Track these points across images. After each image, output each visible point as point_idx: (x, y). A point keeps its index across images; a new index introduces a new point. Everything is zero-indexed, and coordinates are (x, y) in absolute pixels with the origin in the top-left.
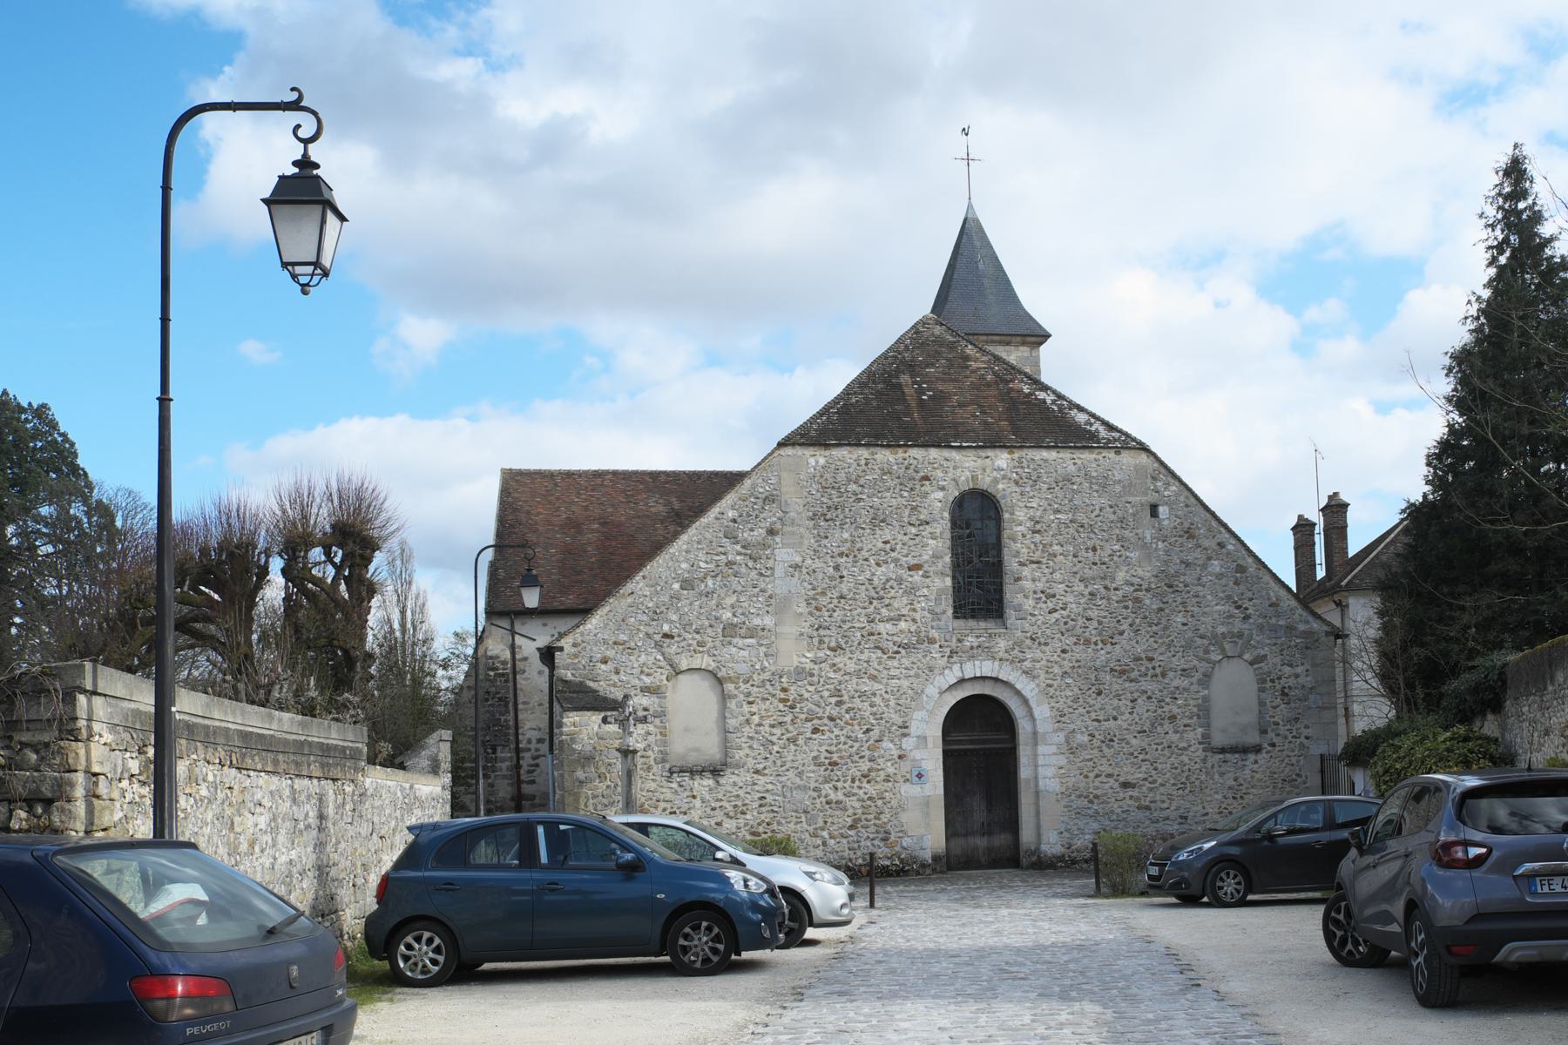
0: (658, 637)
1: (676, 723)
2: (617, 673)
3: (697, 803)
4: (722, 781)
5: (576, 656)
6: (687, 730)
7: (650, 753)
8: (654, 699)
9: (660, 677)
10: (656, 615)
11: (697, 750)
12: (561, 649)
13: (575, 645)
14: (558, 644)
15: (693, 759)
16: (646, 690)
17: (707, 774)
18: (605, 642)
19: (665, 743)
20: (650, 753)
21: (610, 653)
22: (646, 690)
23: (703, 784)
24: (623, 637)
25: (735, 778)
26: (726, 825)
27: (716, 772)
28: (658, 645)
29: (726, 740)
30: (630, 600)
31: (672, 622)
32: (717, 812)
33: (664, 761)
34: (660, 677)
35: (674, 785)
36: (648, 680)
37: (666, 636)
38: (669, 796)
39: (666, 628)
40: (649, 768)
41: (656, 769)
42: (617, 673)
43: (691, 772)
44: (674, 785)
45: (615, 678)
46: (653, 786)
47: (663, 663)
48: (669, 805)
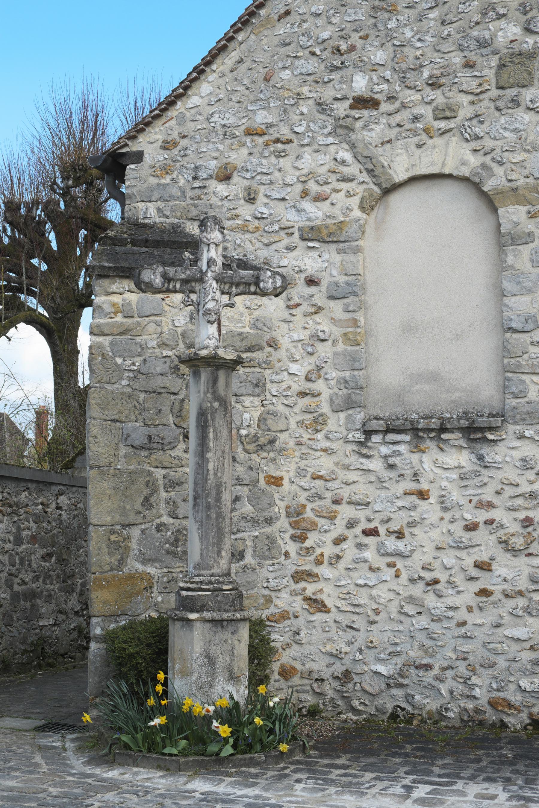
0: (342, 108)
1: (384, 313)
2: (251, 200)
3: (430, 509)
4: (492, 454)
5: (166, 169)
6: (409, 328)
7: (319, 385)
8: (331, 254)
9: (345, 204)
10: (339, 57)
11: (434, 377)
12: (138, 157)
13: (166, 146)
14: (134, 147)
15: (423, 400)
16: (313, 235)
17: (454, 437)
18: (227, 133)
19: (354, 363)
20: (319, 385)
21: (238, 157)
22: (313, 235)
23: (444, 464)
24: (262, 118)
25: (526, 450)
26: (501, 570)
27: (476, 430)
28: (343, 129)
29: (506, 351)
30: (282, 30)
31: (375, 68)
32: (481, 535)
33: (349, 404)
34: (345, 204)
35: (376, 465)
36: (316, 212)
37: (363, 102)
38: (362, 489)
39: (360, 84)
40: (317, 423)
41: (336, 423)
42: (251, 200)
43: (415, 430)
44: (376, 465)
45: (246, 211)
46: (325, 464)
47: (353, 169)
48: (361, 514)
